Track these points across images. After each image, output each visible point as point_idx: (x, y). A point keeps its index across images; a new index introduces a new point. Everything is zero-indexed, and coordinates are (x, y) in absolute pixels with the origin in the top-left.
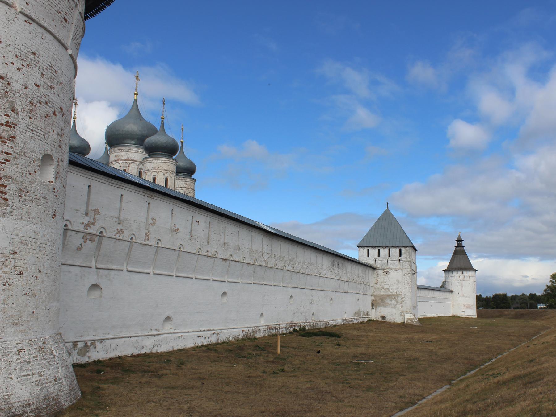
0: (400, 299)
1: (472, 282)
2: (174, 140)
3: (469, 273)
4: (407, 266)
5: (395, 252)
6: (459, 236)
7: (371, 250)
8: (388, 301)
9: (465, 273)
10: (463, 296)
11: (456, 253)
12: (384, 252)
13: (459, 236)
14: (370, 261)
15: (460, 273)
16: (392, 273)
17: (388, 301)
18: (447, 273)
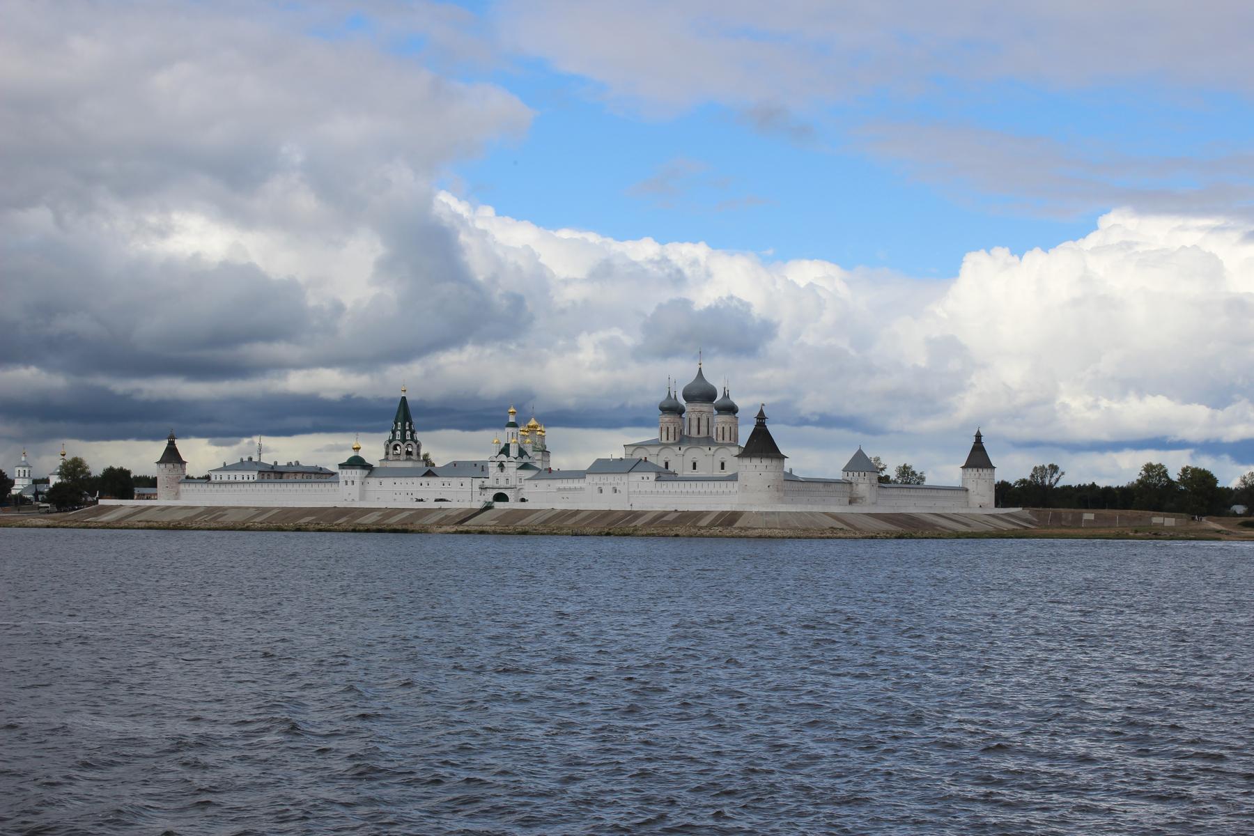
0: (864, 499)
1: (988, 481)
2: (733, 403)
3: (985, 470)
4: (868, 482)
5: (862, 474)
6: (978, 431)
7: (850, 473)
8: (858, 500)
9: (980, 470)
10: (978, 494)
11: (974, 449)
12: (856, 474)
13: (978, 431)
14: (849, 478)
15: (975, 470)
16: (860, 485)
17: (858, 500)
18: (966, 470)
